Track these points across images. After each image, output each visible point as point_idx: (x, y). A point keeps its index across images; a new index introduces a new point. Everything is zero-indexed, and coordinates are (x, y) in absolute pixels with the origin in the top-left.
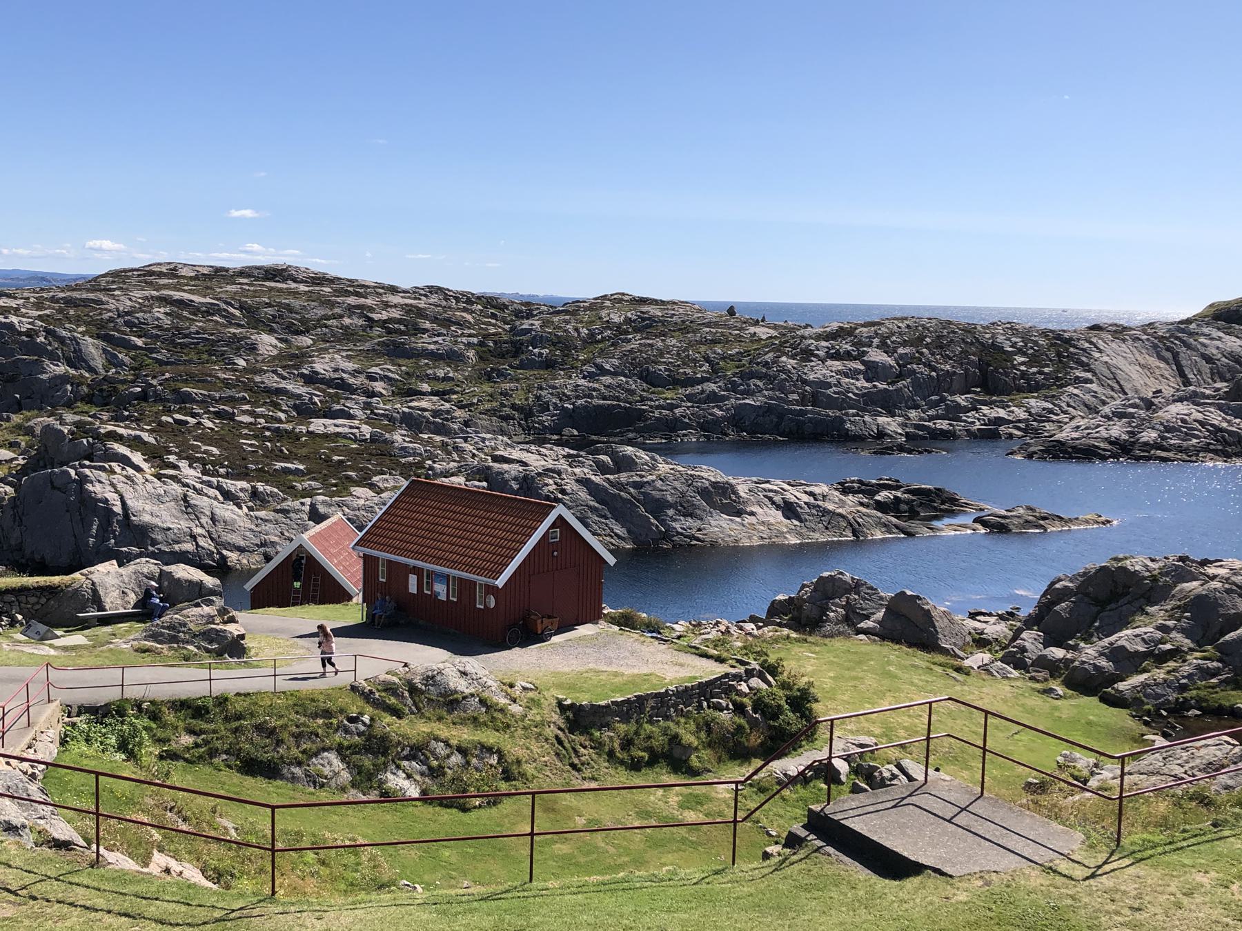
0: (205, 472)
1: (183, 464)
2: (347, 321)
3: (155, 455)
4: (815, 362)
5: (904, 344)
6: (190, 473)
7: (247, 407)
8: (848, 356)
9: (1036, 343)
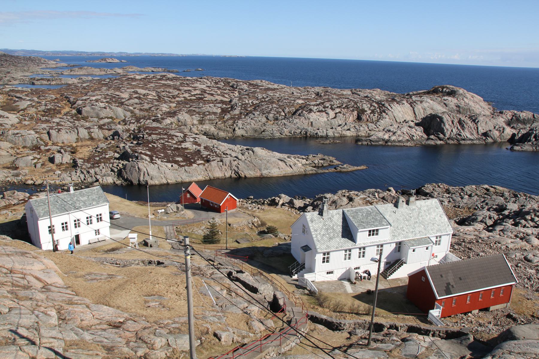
0: (162, 161)
1: (157, 159)
2: (184, 95)
3: (151, 157)
4: (312, 114)
5: (338, 107)
6: (159, 162)
7: (167, 140)
8: (322, 111)
9: (374, 106)
